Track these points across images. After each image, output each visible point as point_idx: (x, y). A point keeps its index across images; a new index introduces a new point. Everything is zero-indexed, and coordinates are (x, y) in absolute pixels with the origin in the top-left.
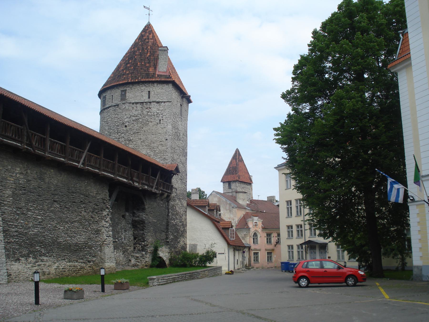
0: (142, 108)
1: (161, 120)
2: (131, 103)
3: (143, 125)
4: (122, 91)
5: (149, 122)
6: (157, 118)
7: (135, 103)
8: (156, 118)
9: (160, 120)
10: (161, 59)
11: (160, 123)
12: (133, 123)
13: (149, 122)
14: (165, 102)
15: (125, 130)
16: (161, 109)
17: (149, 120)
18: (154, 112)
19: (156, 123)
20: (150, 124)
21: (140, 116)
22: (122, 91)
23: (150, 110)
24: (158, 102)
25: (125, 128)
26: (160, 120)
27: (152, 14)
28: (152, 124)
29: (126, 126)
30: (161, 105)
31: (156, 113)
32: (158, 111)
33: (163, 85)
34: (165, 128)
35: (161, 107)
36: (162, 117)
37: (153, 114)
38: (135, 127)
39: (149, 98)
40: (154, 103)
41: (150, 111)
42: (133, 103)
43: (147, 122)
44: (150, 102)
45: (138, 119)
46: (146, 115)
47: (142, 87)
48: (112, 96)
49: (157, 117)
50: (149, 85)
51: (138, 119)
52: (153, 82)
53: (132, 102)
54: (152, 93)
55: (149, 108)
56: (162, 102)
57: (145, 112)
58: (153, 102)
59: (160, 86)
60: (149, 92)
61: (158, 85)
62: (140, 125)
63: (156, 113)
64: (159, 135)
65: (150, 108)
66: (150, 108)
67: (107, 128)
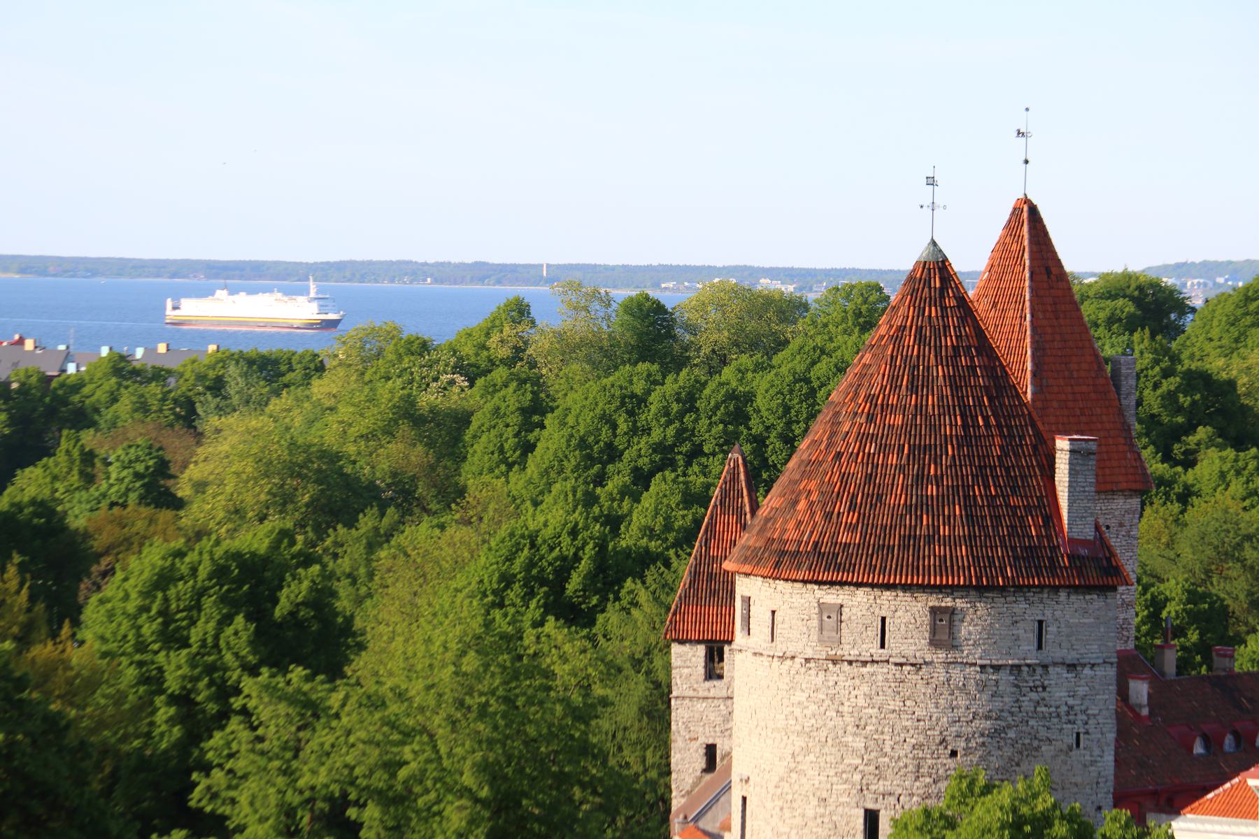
0: (1017, 686)
1: (1081, 735)
2: (975, 664)
3: (1021, 753)
4: (934, 611)
5: (1042, 740)
6: (1070, 726)
7: (992, 667)
8: (1065, 726)
9: (1078, 734)
10: (1077, 489)
11: (1078, 745)
12: (983, 744)
13: (1042, 740)
14: (1093, 665)
15: (952, 766)
16: (1082, 691)
17: (1043, 733)
18: (1058, 703)
19: (1065, 747)
20: (1043, 748)
21: (1010, 719)
22: (934, 611)
23: (1045, 695)
24: (1072, 667)
25: (951, 763)
26: (1078, 734)
27: (945, 207)
28: (1052, 748)
29: (954, 754)
30: (1082, 676)
31: (1066, 708)
32: (1071, 702)
33: (1088, 597)
34: (1093, 763)
35: (1083, 682)
36: (1086, 723)
37: (1053, 709)
38: (991, 759)
39: (1040, 647)
40: (1058, 669)
41: (1043, 699)
42: (983, 667)
43: (1036, 743)
44: (1045, 667)
45: (1004, 730)
46: (1030, 714)
47: (1014, 605)
48: (883, 619)
49: (1070, 722)
50: (1040, 595)
51: (1004, 730)
52: (1055, 589)
53: (979, 662)
54: (1051, 631)
55: (1040, 689)
56: (1084, 665)
57: (1027, 705)
58: (1055, 664)
59: (1077, 600)
60: (1040, 623)
61: (1073, 597)
62: (1008, 752)
63: (1066, 708)
64: (1075, 790)
65: (1044, 688)
66: (1044, 688)
67: (859, 744)
